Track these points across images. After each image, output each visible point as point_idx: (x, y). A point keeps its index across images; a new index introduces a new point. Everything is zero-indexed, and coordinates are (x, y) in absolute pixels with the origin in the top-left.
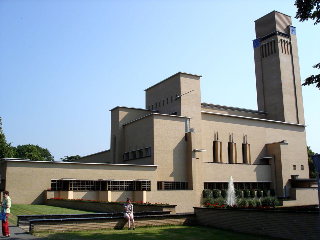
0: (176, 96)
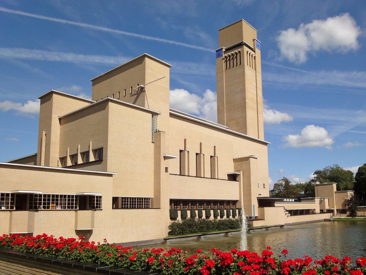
0: (138, 85)
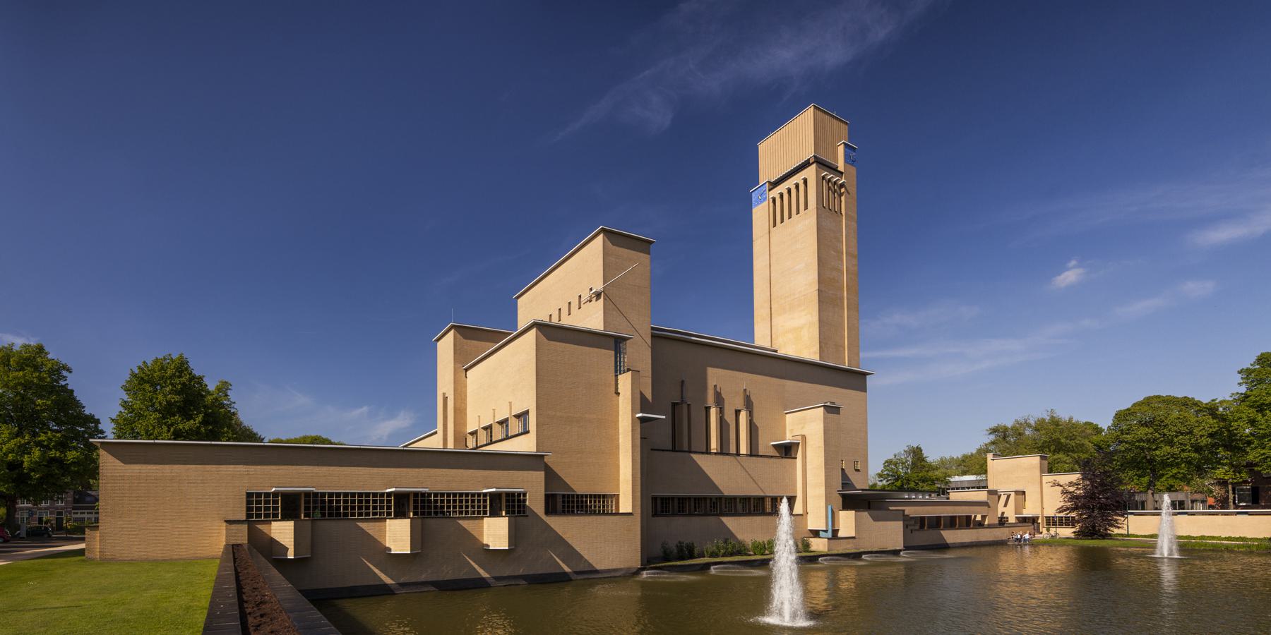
0: (591, 289)
